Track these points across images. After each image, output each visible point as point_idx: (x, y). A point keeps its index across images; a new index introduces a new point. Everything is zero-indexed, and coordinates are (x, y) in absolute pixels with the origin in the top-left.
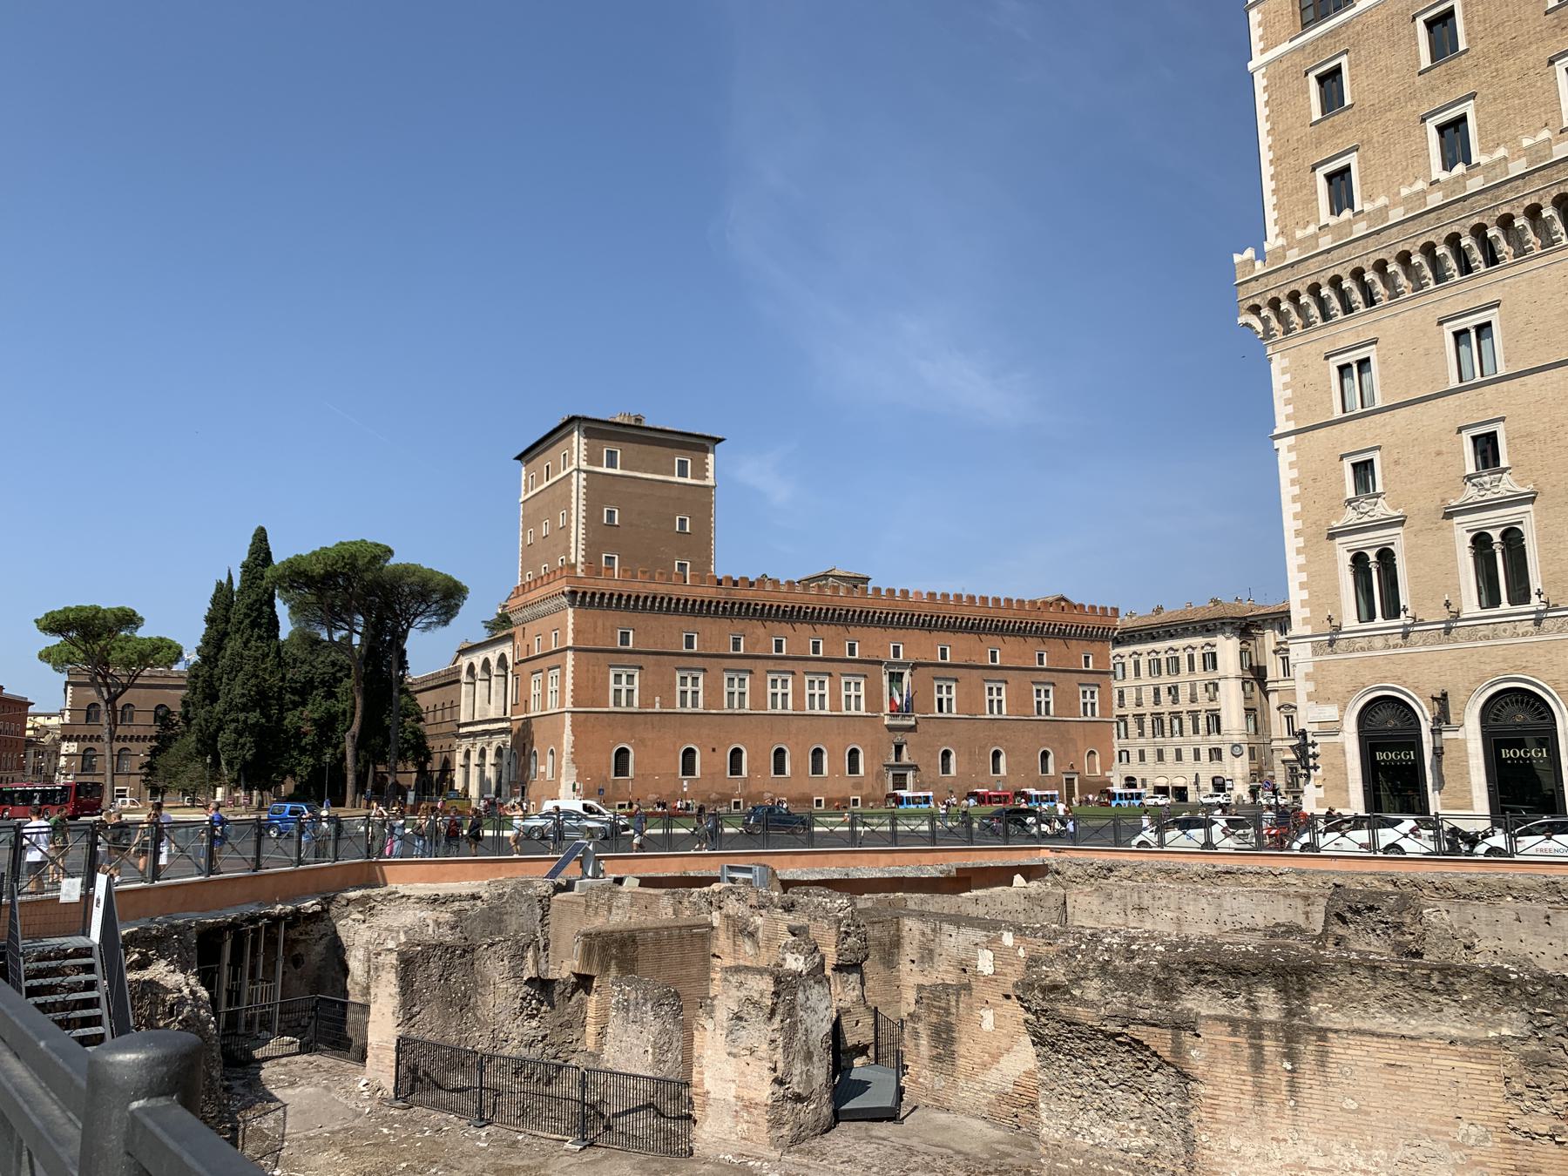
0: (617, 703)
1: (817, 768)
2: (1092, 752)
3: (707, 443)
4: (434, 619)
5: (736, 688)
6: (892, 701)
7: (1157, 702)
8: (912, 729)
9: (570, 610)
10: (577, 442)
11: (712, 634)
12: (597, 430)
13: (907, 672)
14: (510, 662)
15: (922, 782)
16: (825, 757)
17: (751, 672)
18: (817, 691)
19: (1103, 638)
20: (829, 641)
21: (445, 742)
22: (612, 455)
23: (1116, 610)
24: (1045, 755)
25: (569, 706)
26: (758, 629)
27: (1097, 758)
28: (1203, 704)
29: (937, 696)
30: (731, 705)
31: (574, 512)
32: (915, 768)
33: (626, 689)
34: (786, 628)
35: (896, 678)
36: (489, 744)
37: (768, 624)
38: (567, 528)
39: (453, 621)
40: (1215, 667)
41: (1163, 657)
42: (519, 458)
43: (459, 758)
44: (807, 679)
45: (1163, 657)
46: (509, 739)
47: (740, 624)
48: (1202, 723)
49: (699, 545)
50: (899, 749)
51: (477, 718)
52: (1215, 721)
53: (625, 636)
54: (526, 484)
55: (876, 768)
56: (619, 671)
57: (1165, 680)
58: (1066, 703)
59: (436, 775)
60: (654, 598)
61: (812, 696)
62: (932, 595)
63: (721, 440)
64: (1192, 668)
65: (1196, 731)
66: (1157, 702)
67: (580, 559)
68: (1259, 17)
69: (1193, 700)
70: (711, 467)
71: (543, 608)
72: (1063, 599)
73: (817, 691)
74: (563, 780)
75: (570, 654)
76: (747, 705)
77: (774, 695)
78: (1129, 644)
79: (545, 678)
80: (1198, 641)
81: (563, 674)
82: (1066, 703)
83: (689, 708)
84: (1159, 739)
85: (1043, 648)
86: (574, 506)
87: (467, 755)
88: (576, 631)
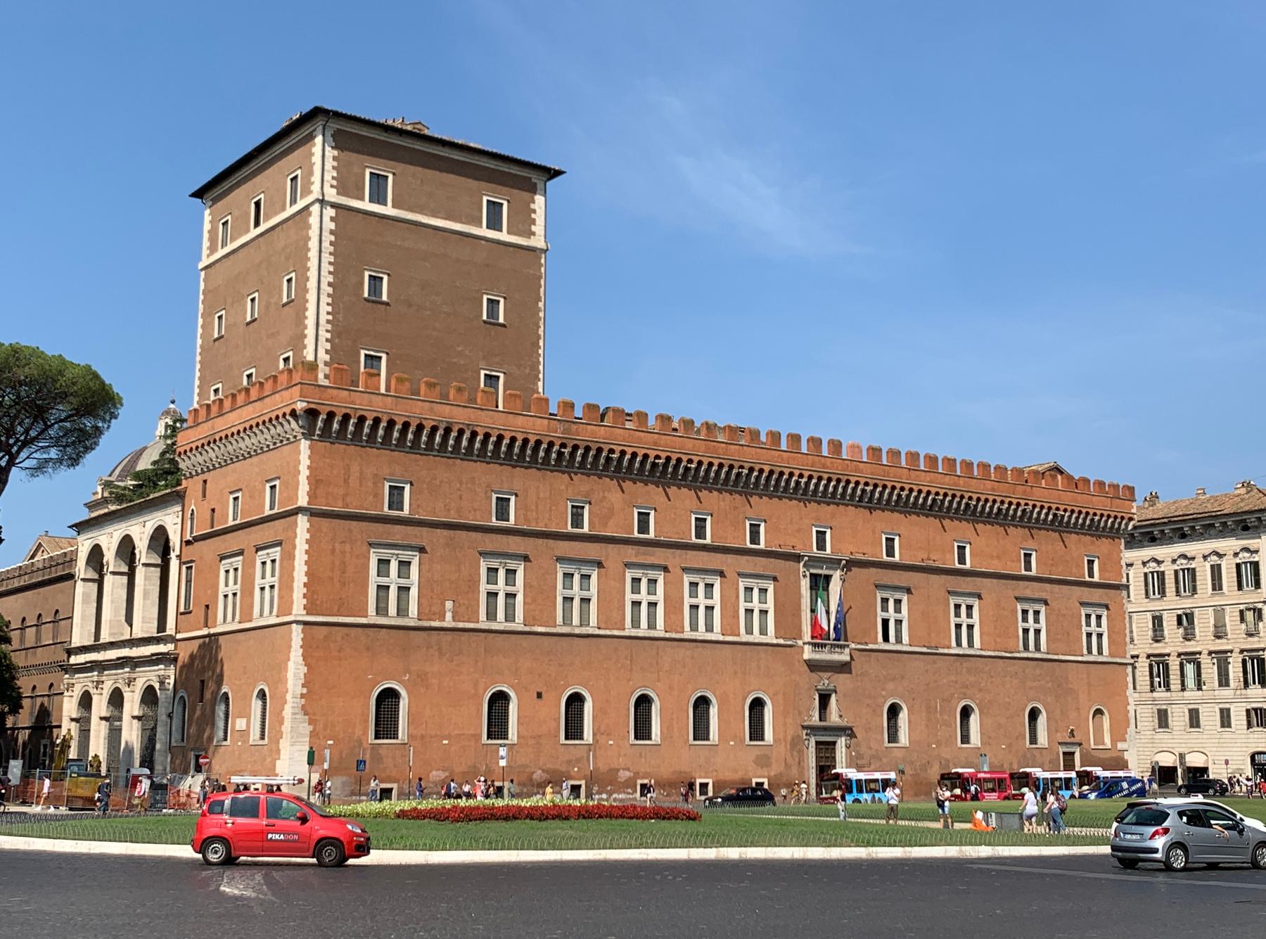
0: (381, 610)
1: (701, 731)
2: (1099, 712)
3: (535, 177)
4: (53, 453)
5: (576, 591)
6: (815, 624)
7: (1158, 637)
8: (844, 668)
9: (304, 445)
10: (320, 153)
11: (538, 498)
12: (359, 136)
13: (837, 576)
14: (175, 540)
15: (859, 756)
16: (714, 711)
17: (600, 565)
18: (701, 601)
19: (1113, 533)
20: (722, 517)
21: (41, 682)
22: (379, 180)
23: (1131, 490)
24: (1034, 714)
25: (298, 610)
26: (610, 493)
27: (1106, 720)
29: (880, 615)
30: (567, 620)
31: (313, 274)
32: (848, 731)
33: (397, 585)
34: (654, 494)
35: (819, 584)
36: (130, 682)
37: (627, 485)
38: (296, 305)
39: (89, 458)
40: (1257, 585)
41: (1169, 570)
42: (199, 194)
43: (70, 707)
44: (687, 579)
45: (1169, 570)
46: (171, 673)
47: (583, 484)
48: (1235, 670)
49: (517, 345)
50: (824, 700)
51: (105, 637)
53: (396, 492)
54: (213, 236)
55: (790, 733)
56: (385, 553)
57: (1172, 604)
58: (1063, 632)
59: (23, 736)
60: (448, 431)
61: (694, 607)
62: (875, 451)
63: (558, 173)
64: (1217, 585)
65: (1224, 681)
66: (1158, 637)
67: (323, 356)
69: (1219, 634)
70: (539, 217)
71: (247, 443)
72: (1058, 470)
73: (701, 601)
74: (284, 744)
75: (302, 522)
76: (593, 620)
77: (637, 604)
78: (1201, 536)
79: (249, 565)
80: (1228, 545)
81: (289, 557)
82: (1063, 632)
83: (500, 624)
84: (1160, 694)
85: (1031, 544)
86: (313, 264)
87: (86, 701)
88: (314, 481)
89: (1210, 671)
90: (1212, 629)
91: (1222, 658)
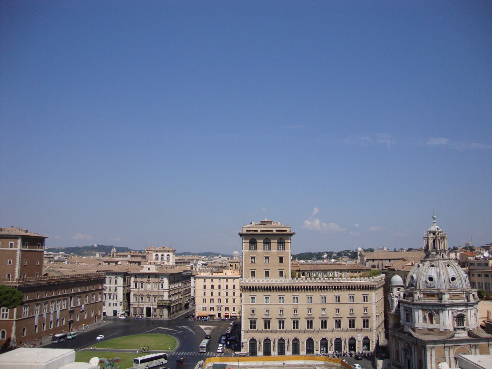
25: (15, 319)
28: (113, 292)
48: (112, 297)
52: (116, 296)
64: (110, 282)
68: (244, 245)
89: (108, 296)
90: (109, 290)
91: (110, 295)
